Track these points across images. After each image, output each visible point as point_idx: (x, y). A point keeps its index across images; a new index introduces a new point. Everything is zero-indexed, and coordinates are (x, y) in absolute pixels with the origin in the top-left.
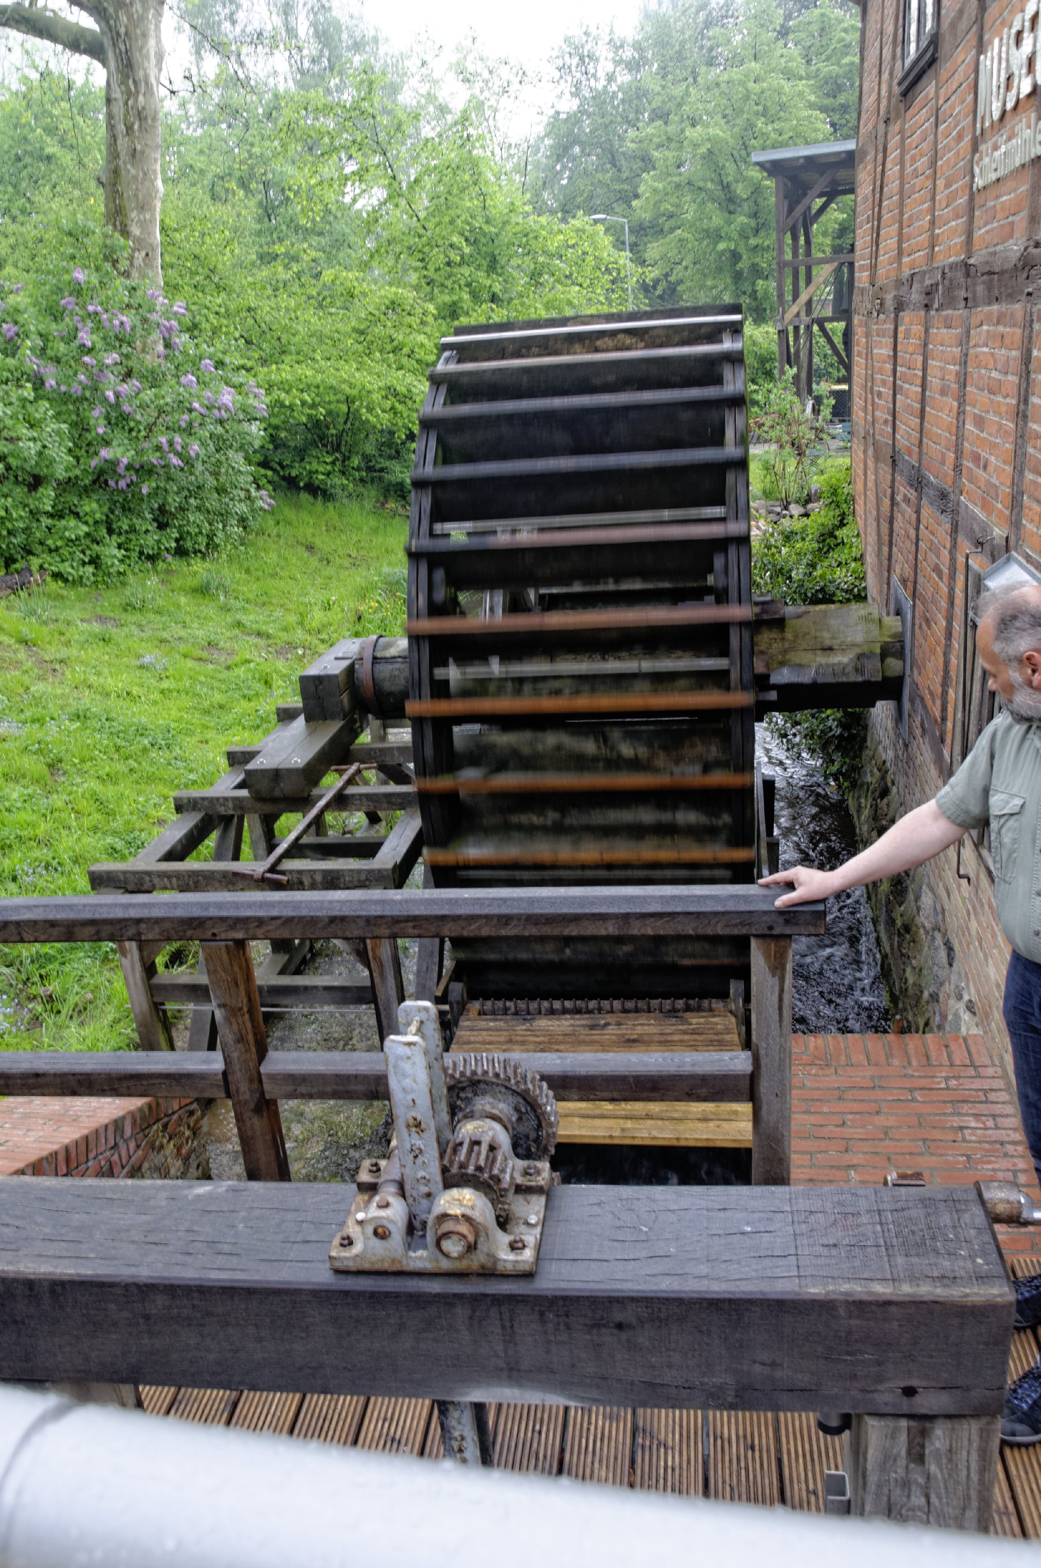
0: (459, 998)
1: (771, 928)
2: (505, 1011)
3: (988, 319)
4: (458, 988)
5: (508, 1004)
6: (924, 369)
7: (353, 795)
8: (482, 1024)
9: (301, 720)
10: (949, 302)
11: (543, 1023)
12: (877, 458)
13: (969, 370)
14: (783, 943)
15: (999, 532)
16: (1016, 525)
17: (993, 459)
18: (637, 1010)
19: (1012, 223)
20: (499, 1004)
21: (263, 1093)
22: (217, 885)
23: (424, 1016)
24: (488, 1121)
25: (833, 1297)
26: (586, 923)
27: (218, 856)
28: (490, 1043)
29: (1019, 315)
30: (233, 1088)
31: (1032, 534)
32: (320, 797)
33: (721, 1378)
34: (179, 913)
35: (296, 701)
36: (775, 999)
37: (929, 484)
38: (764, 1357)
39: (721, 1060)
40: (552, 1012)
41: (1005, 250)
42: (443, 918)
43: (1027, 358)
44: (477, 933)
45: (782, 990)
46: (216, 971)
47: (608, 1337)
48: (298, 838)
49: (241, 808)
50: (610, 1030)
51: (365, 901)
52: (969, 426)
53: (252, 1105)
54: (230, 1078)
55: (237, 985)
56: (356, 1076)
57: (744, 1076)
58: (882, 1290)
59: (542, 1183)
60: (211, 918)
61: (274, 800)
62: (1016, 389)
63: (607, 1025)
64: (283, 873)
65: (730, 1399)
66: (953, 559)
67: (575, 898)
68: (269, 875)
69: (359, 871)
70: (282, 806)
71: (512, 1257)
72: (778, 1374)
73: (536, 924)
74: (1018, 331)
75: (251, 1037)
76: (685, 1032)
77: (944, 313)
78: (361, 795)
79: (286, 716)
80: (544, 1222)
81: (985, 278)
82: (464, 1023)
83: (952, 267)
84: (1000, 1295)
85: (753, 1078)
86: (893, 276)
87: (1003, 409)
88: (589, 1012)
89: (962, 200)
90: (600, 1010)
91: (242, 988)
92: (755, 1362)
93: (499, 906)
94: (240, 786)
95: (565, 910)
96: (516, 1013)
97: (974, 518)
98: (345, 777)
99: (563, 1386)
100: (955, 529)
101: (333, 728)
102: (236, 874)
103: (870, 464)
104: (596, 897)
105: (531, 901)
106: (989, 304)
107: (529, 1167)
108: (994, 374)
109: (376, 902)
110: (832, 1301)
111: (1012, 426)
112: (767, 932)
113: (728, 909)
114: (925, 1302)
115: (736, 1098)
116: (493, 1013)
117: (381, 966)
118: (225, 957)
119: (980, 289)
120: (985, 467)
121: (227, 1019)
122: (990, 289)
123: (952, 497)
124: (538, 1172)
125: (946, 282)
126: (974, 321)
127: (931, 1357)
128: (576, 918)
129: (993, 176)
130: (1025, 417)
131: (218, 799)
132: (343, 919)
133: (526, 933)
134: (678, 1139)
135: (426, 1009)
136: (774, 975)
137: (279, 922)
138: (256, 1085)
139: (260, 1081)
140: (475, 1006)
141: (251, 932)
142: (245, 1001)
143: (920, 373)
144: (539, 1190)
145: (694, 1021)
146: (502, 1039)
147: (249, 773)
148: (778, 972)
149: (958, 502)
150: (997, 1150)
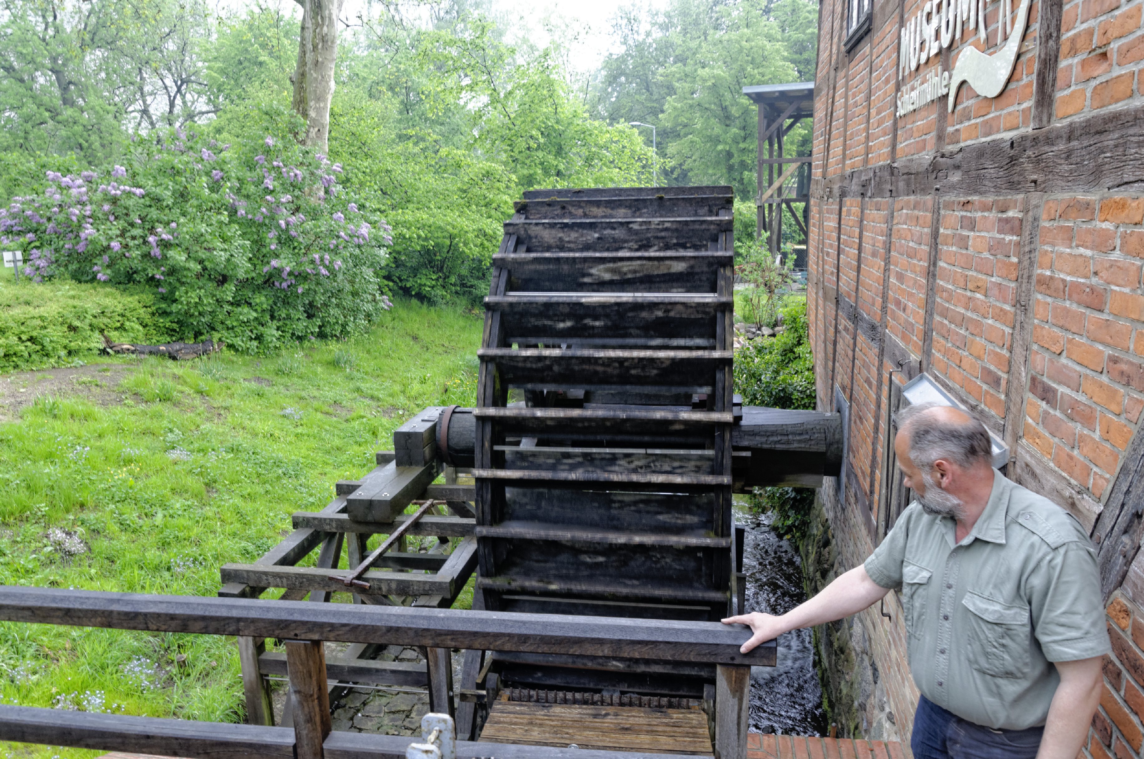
0: (494, 686)
2: (529, 699)
3: (907, 206)
4: (494, 677)
5: (532, 692)
6: (860, 238)
7: (426, 523)
8: (511, 708)
9: (393, 465)
10: (879, 192)
11: (558, 710)
12: (825, 298)
13: (893, 240)
14: (742, 671)
15: (914, 357)
16: (927, 352)
17: (910, 304)
19: (925, 140)
20: (525, 692)
22: (316, 586)
23: (442, 726)
26: (587, 646)
27: (322, 564)
28: (515, 724)
29: (930, 204)
32: (402, 523)
35: (390, 449)
37: (862, 319)
40: (565, 701)
41: (920, 158)
42: (475, 634)
43: (935, 235)
45: (740, 709)
48: (381, 555)
49: (342, 528)
50: (609, 719)
51: (415, 617)
52: (893, 280)
55: (310, 677)
60: (295, 622)
61: (367, 523)
62: (927, 255)
63: (607, 715)
64: (367, 580)
66: (880, 374)
67: (579, 624)
68: (356, 581)
69: (425, 583)
70: (372, 528)
74: (929, 215)
76: (667, 725)
78: (432, 523)
79: (383, 460)
81: (905, 177)
82: (496, 706)
83: (881, 168)
86: (839, 172)
88: (594, 703)
89: (889, 123)
90: (602, 702)
93: (520, 627)
94: (343, 511)
95: (571, 634)
96: (537, 701)
97: (896, 345)
98: (422, 509)
101: (416, 471)
102: (331, 579)
103: (821, 302)
104: (596, 625)
105: (545, 625)
106: (908, 195)
108: (911, 244)
109: (425, 618)
111: (924, 281)
113: (700, 641)
116: (520, 699)
117: (436, 657)
119: (901, 185)
120: (904, 310)
122: (908, 184)
123: (880, 329)
125: (877, 179)
126: (897, 206)
128: (579, 641)
129: (911, 108)
130: (934, 275)
131: (325, 519)
132: (398, 629)
135: (445, 721)
137: (347, 628)
140: (506, 693)
141: (325, 635)
143: (857, 241)
145: (675, 716)
146: (525, 721)
147: (349, 501)
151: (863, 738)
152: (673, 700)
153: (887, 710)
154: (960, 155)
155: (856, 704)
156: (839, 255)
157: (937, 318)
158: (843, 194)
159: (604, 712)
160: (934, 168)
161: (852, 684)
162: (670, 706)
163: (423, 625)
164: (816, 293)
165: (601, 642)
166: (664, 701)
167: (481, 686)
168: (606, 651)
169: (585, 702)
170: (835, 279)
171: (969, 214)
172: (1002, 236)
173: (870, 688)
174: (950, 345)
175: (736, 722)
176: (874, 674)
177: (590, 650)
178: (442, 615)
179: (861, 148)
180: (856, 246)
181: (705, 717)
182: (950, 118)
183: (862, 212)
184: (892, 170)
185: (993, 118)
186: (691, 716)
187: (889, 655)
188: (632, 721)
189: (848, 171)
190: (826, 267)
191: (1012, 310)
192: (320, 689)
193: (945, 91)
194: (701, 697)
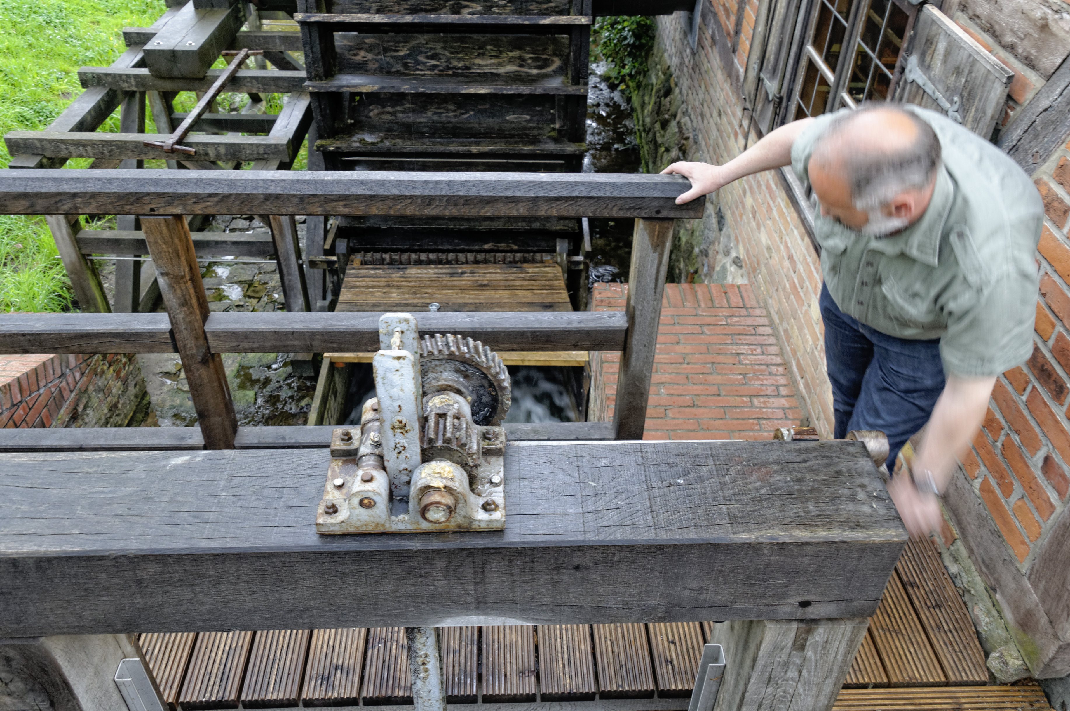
1: (658, 212)
2: (382, 261)
5: (384, 256)
8: (365, 272)
11: (413, 271)
18: (486, 261)
20: (378, 256)
21: (208, 348)
24: (452, 394)
25: (761, 540)
26: (500, 205)
30: (180, 344)
33: (657, 600)
34: (114, 188)
36: (654, 271)
38: (695, 584)
39: (600, 318)
40: (419, 263)
42: (372, 197)
44: (402, 212)
46: (156, 243)
47: (566, 576)
51: (298, 181)
53: (199, 358)
54: (177, 336)
55: (178, 255)
56: (293, 333)
57: (621, 331)
58: (801, 534)
59: (501, 446)
60: (148, 194)
63: (463, 273)
65: (660, 615)
71: (481, 516)
72: (703, 596)
73: (456, 205)
75: (194, 301)
80: (506, 480)
84: (897, 536)
85: (628, 333)
88: (449, 262)
90: (457, 261)
91: (183, 258)
92: (685, 588)
93: (423, 188)
95: (482, 193)
96: (391, 263)
99: (523, 613)
104: (509, 182)
105: (451, 184)
107: (488, 433)
109: (309, 182)
110: (760, 543)
112: (654, 215)
113: (624, 195)
114: (835, 542)
115: (612, 348)
116: (372, 262)
118: (165, 230)
121: (171, 286)
124: (496, 436)
127: (829, 580)
128: (491, 201)
132: (278, 196)
133: (447, 213)
134: (523, 361)
136: (655, 251)
137: (216, 199)
138: (201, 342)
139: (206, 339)
140: (358, 258)
141: (189, 208)
142: (187, 270)
144: (498, 452)
148: (659, 249)
150: (764, 371)
151: (703, 282)
152: (527, 255)
153: (734, 254)
155: (696, 250)
159: (460, 271)
161: (693, 233)
162: (525, 261)
163: (309, 190)
165: (515, 200)
166: (518, 256)
167: (331, 251)
168: (521, 210)
169: (439, 262)
173: (712, 235)
175: (654, 277)
176: (719, 222)
177: (503, 210)
178: (329, 178)
181: (560, 269)
186: (547, 269)
187: (742, 203)
188: (488, 277)
192: (191, 269)
194: (554, 251)
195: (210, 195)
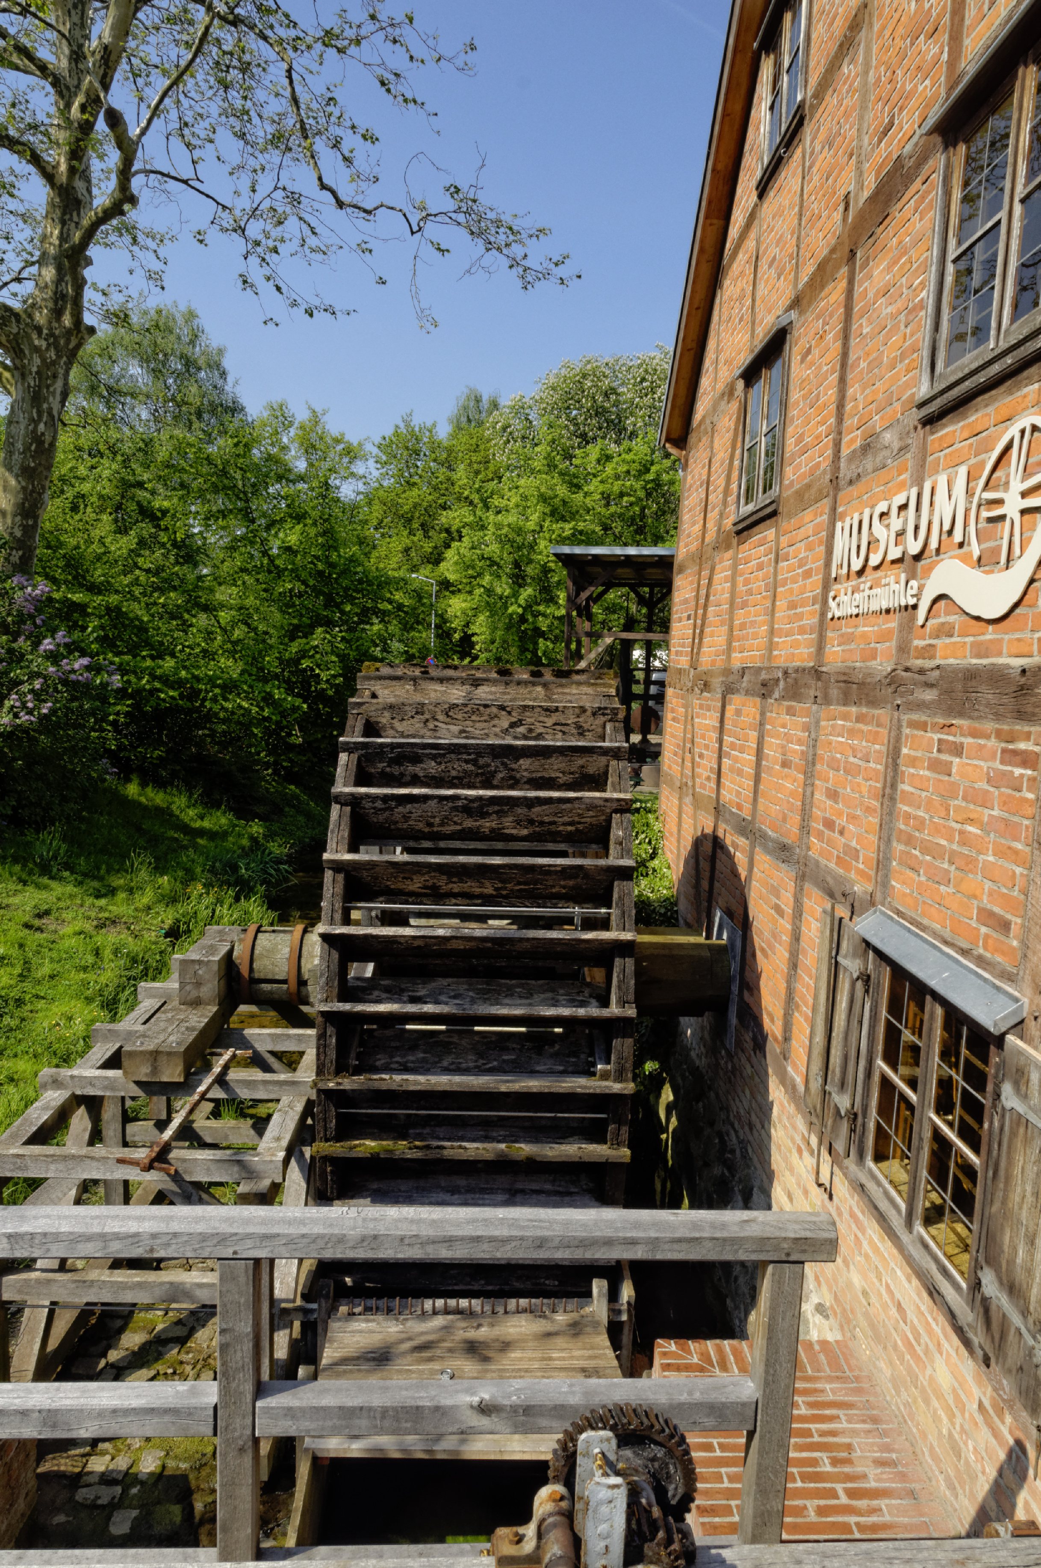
1: (788, 1255)
3: (845, 717)
13: (820, 752)
15: (860, 888)
16: (885, 884)
31: (905, 895)
37: (764, 836)
43: (894, 754)
74: (884, 732)
77: (786, 703)
87: (865, 790)
97: (829, 872)
100: (801, 878)
103: (688, 809)
112: (784, 1258)
120: (841, 833)
129: (855, 611)
130: (892, 799)
149: (806, 857)
154: (937, 673)
156: (720, 758)
157: (898, 847)
158: (729, 690)
160: (893, 681)
164: (680, 799)
170: (713, 785)
171: (951, 738)
172: (1009, 768)
174: (923, 878)
179: (762, 641)
180: (754, 752)
182: (918, 631)
183: (763, 714)
184: (817, 673)
185: (991, 641)
189: (736, 664)
190: (697, 770)
191: (1028, 849)
193: (912, 601)
195: (303, 1236)
